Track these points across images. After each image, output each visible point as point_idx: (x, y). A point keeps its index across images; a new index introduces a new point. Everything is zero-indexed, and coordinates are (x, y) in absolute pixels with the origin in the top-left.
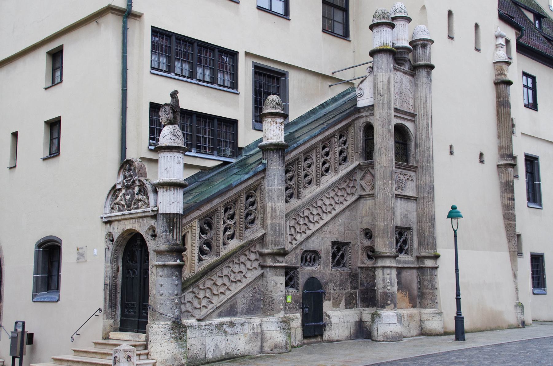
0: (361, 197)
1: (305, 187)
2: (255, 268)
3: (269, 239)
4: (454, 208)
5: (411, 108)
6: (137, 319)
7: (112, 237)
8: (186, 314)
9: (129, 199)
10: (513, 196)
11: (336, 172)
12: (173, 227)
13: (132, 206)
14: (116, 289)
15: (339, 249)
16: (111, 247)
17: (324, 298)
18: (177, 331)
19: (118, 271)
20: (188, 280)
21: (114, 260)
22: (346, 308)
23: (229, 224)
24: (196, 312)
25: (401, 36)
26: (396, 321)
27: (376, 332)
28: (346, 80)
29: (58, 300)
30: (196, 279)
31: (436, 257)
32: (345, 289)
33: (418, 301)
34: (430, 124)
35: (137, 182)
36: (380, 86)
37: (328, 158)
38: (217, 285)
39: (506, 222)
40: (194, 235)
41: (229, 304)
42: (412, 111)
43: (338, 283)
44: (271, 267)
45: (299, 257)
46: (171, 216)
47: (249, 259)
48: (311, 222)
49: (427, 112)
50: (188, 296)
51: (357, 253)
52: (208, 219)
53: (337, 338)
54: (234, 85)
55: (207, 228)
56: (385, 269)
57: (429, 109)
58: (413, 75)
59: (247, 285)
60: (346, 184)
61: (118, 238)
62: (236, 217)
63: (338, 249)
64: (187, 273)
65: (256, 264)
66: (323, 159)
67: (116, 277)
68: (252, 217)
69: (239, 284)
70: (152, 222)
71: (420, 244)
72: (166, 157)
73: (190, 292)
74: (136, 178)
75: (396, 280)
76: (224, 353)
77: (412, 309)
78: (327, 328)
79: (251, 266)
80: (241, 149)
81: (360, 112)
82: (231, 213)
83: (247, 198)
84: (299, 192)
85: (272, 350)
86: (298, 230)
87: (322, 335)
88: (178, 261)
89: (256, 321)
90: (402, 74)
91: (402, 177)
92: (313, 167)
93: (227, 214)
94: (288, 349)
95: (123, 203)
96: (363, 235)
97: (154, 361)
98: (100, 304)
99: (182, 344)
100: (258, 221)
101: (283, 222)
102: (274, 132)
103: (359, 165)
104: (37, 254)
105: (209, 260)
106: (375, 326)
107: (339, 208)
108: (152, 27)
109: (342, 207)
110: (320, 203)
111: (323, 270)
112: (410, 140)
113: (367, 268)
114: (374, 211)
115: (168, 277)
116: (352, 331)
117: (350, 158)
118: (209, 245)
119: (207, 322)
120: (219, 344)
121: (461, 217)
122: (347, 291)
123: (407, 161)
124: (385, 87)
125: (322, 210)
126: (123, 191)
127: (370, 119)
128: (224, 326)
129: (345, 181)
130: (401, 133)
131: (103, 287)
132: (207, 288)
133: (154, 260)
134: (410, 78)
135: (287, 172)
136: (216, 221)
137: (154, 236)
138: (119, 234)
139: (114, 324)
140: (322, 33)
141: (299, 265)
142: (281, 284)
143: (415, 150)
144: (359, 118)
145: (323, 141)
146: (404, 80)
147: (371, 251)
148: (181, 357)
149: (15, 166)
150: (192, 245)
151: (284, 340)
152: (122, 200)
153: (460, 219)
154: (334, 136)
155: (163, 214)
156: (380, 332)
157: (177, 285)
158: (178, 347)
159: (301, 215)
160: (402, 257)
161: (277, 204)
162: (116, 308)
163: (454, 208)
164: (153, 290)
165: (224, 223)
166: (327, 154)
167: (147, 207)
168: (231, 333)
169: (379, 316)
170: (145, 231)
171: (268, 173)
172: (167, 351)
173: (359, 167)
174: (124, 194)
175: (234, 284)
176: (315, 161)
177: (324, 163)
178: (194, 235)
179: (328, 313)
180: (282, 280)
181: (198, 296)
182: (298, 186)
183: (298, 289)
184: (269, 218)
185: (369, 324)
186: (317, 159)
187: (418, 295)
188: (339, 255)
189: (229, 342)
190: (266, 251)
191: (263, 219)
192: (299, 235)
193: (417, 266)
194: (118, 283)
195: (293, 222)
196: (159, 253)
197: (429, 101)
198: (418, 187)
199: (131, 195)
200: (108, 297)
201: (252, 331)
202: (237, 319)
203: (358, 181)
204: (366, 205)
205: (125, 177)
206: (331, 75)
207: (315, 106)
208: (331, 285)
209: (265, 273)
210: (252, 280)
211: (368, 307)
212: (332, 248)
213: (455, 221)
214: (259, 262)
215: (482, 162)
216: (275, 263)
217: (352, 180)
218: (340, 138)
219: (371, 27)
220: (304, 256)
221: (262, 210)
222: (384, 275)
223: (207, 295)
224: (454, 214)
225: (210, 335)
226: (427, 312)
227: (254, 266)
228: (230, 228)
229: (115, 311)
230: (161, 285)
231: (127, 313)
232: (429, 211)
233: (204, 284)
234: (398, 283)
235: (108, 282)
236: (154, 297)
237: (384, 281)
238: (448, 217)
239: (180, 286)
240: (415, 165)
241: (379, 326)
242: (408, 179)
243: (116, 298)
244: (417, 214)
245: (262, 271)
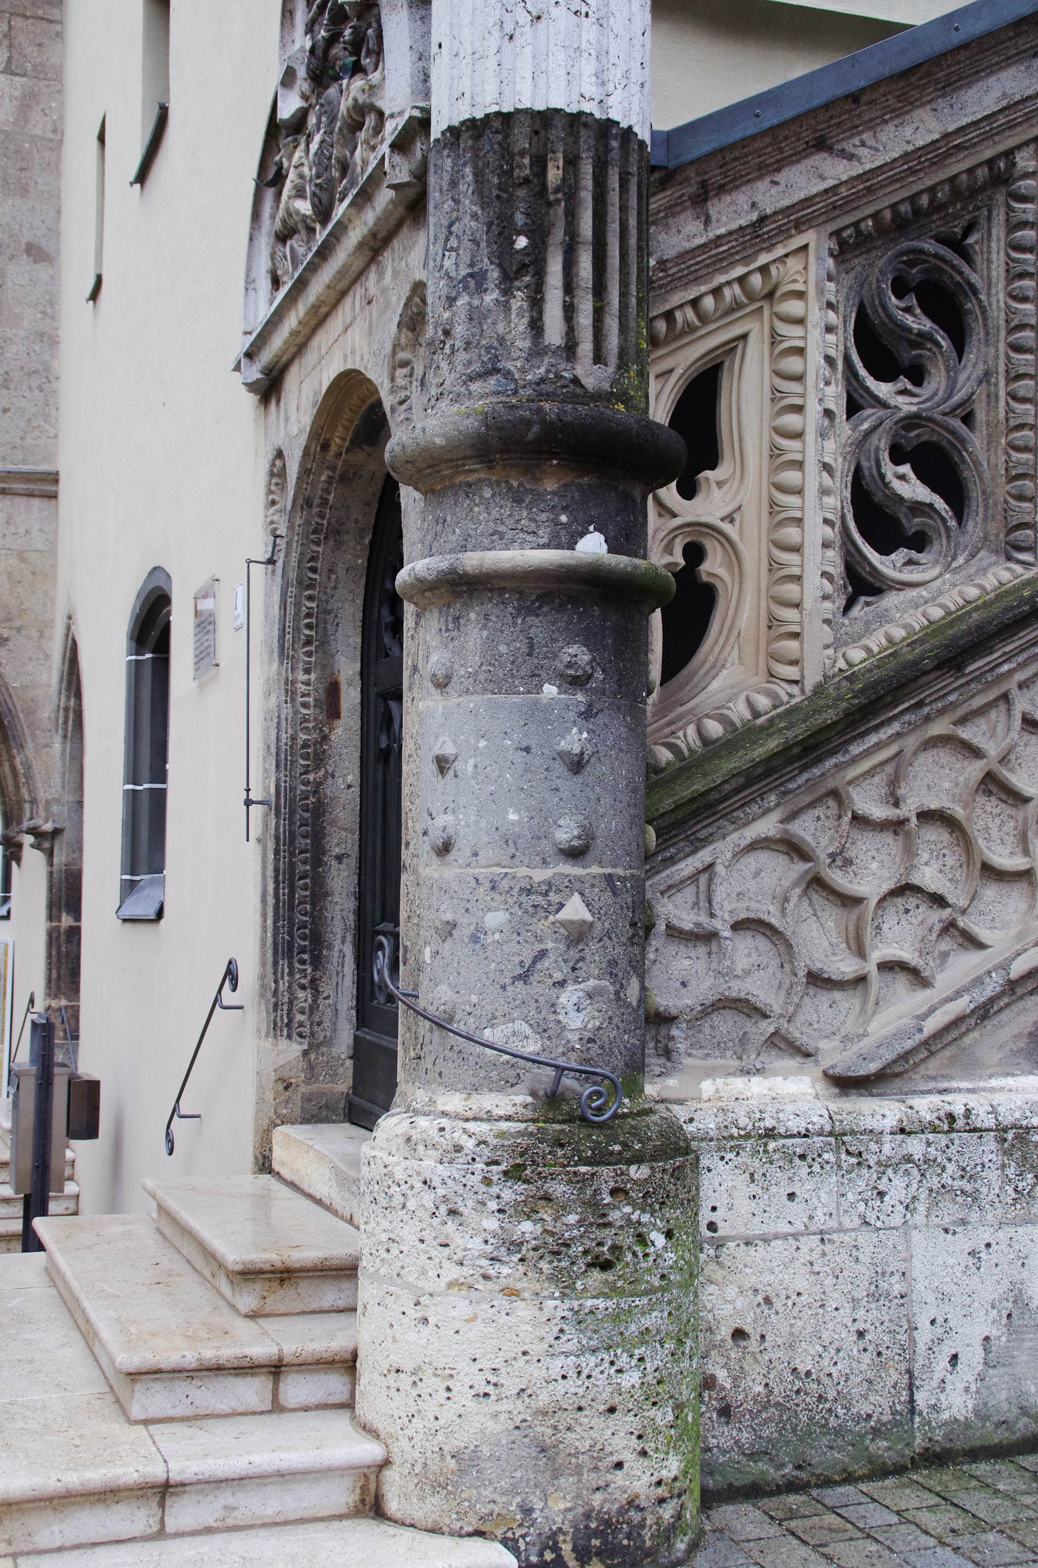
8: (725, 1023)
12: (539, 236)
14: (318, 836)
18: (559, 1189)
19: (331, 706)
20: (741, 736)
24: (823, 1019)
29: (160, 914)
30: (800, 731)
40: (792, 364)
46: (521, 140)
50: (742, 872)
52: (930, 246)
55: (919, 323)
64: (734, 683)
67: (317, 754)
97: (369, 1451)
99: (616, 1317)
105: (934, 590)
115: (496, 685)
119: (925, 1106)
132: (926, 816)
136: (998, 272)
138: (303, 440)
139: (311, 1068)
148: (618, 1437)
150: (775, 452)
157: (577, 765)
158: (572, 1341)
162: (317, 961)
172: (470, 1378)
178: (792, 364)
181: (838, 878)
194: (329, 789)
223: (929, 877)
225: (950, 1211)
229: (314, 985)
233: (894, 783)
239: (614, 774)
243: (319, 894)
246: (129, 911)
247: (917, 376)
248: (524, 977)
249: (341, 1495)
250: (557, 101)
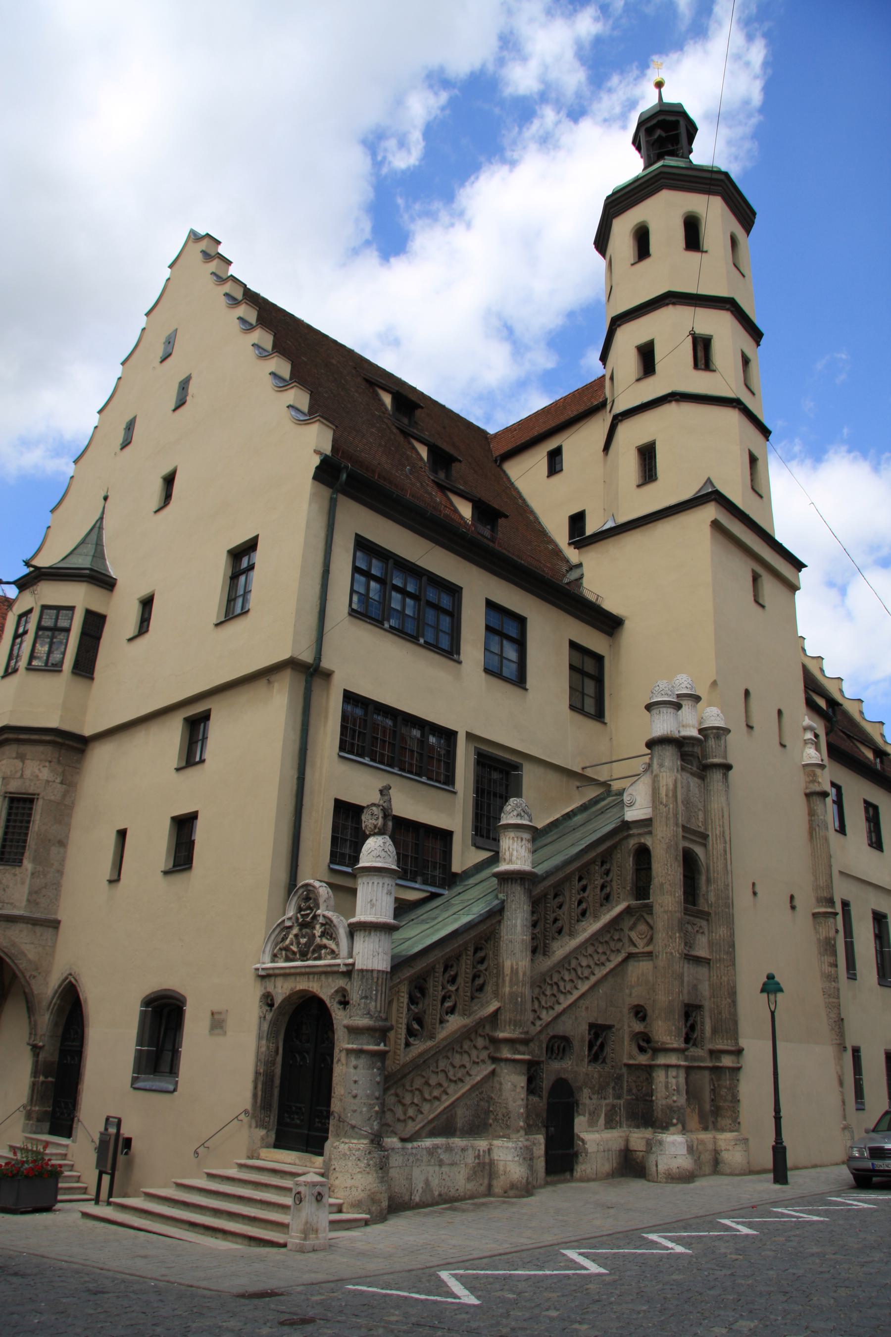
0: (630, 956)
1: (553, 939)
2: (483, 1061)
3: (505, 1016)
4: (771, 977)
5: (700, 824)
6: (306, 1132)
7: (272, 1000)
9: (305, 944)
10: (836, 960)
11: (596, 917)
13: (310, 955)
14: (272, 1081)
15: (599, 1033)
16: (269, 1016)
17: (577, 1112)
18: (376, 1155)
21: (272, 1034)
22: (606, 1128)
23: (449, 991)
24: (399, 1127)
25: (686, 723)
26: (684, 1151)
27: (654, 1168)
28: (602, 779)
29: (175, 1090)
31: (739, 1052)
32: (605, 1099)
33: (711, 1119)
34: (728, 849)
35: (321, 920)
36: (663, 792)
37: (586, 895)
38: (429, 1085)
39: (827, 1000)
41: (445, 1116)
42: (702, 830)
43: (596, 1088)
44: (507, 1060)
45: (544, 1046)
46: (375, 975)
47: (475, 1047)
48: (562, 992)
49: (724, 832)
51: (623, 1042)
53: (594, 1176)
54: (450, 780)
55: (419, 995)
56: (670, 1069)
57: (727, 828)
58: (702, 778)
59: (473, 1087)
60: (609, 936)
61: (282, 1002)
62: (460, 980)
63: (597, 1036)
65: (484, 1055)
66: (579, 897)
67: (274, 1063)
68: (480, 981)
69: (460, 1084)
70: (341, 982)
71: (714, 1031)
72: (370, 884)
73: (392, 1094)
74: (319, 912)
75: (685, 1087)
76: (436, 1193)
77: (703, 1132)
78: (581, 1159)
79: (478, 1057)
80: (455, 875)
81: (629, 828)
82: (452, 973)
83: (475, 952)
84: (546, 946)
85: (505, 1192)
86: (543, 1003)
87: (572, 1170)
88: (382, 1044)
89: (482, 1144)
90: (688, 775)
91: (690, 928)
92: (565, 908)
93: (447, 975)
94: (526, 1190)
95: (294, 948)
96: (632, 1015)
97: (340, 1201)
98: (247, 1104)
100: (489, 989)
101: (527, 991)
102: (516, 855)
103: (628, 907)
104: (143, 1015)
106: (652, 1159)
107: (600, 972)
108: (345, 690)
109: (605, 970)
110: (574, 963)
111: (574, 1067)
112: (699, 872)
113: (639, 1067)
114: (651, 978)
115: (368, 1069)
116: (615, 1165)
117: (616, 896)
118: (420, 1022)
119: (415, 1144)
120: (430, 1179)
121: (781, 990)
122: (607, 1101)
123: (694, 904)
124: (671, 794)
125: (577, 974)
126: (295, 930)
127: (648, 841)
128: (439, 1151)
129: (609, 932)
130: (690, 865)
131: (249, 1077)
133: (343, 1042)
134: (699, 781)
135: (533, 913)
137: (344, 1003)
138: (284, 996)
140: (569, 710)
141: (543, 1059)
142: (522, 1087)
143: (707, 888)
144: (629, 836)
145: (580, 869)
146: (692, 784)
147: (643, 1040)
149: (118, 880)
151: (525, 1175)
152: (292, 944)
153: (779, 995)
154: (594, 862)
155: (362, 971)
156: (662, 1168)
157: (378, 1083)
159: (548, 980)
160: (693, 1051)
161: (520, 963)
162: (270, 1111)
163: (771, 977)
164: (339, 1089)
165: (443, 988)
166: (584, 889)
167: (335, 958)
168: (447, 1162)
169: (660, 1143)
170: (330, 994)
171: (507, 914)
172: (361, 1187)
173: (628, 911)
174: (296, 936)
175: (452, 1085)
176: (568, 899)
177: (580, 902)
179: (582, 1135)
180: (521, 1081)
181: (403, 1101)
182: (545, 936)
183: (540, 1097)
184: (507, 983)
185: (641, 1154)
186: (571, 896)
187: (712, 1111)
188: (598, 1043)
189: (444, 1177)
190: (501, 1035)
191: (497, 985)
192: (544, 1012)
193: (710, 1064)
195: (537, 990)
196: (354, 1031)
197: (726, 816)
198: (711, 944)
199: (309, 939)
200: (260, 1093)
201: (477, 1161)
202: (457, 1142)
203: (626, 931)
204: (639, 969)
205: (300, 909)
206: (580, 771)
207: (557, 816)
208: (586, 1092)
209: (498, 1070)
210: (478, 1078)
211: (638, 1127)
212: (589, 1034)
213: (772, 997)
214: (488, 1052)
215: (793, 908)
216: (514, 1053)
217: (616, 930)
218: (602, 865)
219: (649, 707)
220: (550, 1045)
221: (495, 971)
222: (667, 1077)
223: (416, 1101)
224: (771, 987)
226: (725, 1138)
227: (481, 1057)
228: (450, 997)
230: (355, 1082)
231: (288, 1120)
232: (728, 980)
234: (687, 1092)
235: (262, 1071)
236: (341, 1100)
237: (667, 1087)
238: (762, 991)
240: (706, 909)
241: (659, 1158)
242: (697, 931)
244: (709, 985)
245: (493, 1066)
246: (136, 1085)
247: (417, 1004)
248: (369, 1120)
249: (335, 1209)
250: (380, 968)
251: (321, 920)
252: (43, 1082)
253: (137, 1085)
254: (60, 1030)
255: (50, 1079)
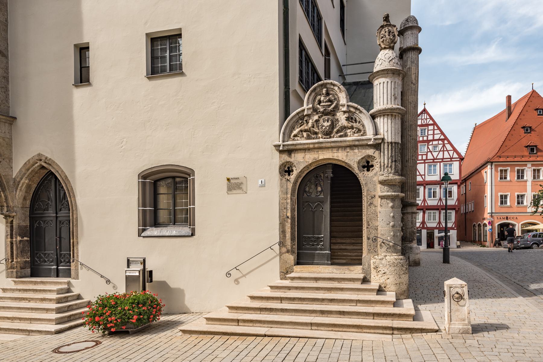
61: (304, 168)
138: (306, 164)
152: (313, 127)
167: (362, 135)
174: (317, 121)
251: (345, 109)
252: (20, 241)
253: (143, 235)
254: (28, 202)
255: (25, 238)
